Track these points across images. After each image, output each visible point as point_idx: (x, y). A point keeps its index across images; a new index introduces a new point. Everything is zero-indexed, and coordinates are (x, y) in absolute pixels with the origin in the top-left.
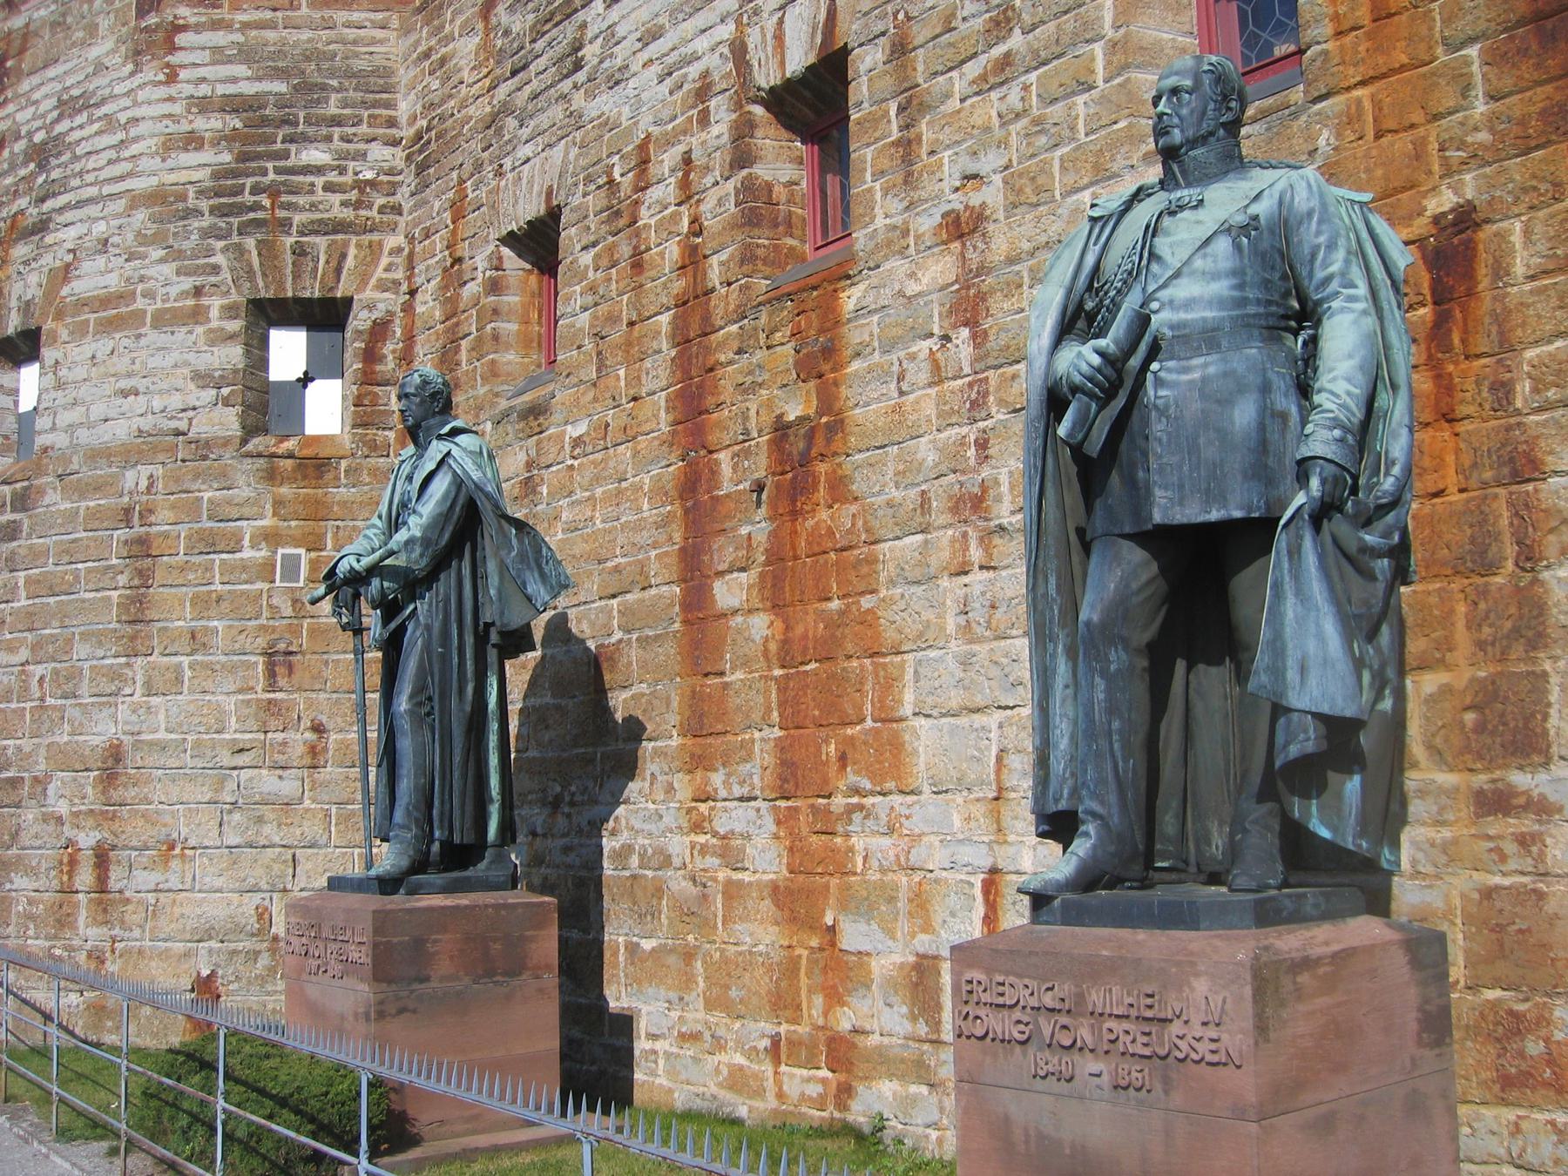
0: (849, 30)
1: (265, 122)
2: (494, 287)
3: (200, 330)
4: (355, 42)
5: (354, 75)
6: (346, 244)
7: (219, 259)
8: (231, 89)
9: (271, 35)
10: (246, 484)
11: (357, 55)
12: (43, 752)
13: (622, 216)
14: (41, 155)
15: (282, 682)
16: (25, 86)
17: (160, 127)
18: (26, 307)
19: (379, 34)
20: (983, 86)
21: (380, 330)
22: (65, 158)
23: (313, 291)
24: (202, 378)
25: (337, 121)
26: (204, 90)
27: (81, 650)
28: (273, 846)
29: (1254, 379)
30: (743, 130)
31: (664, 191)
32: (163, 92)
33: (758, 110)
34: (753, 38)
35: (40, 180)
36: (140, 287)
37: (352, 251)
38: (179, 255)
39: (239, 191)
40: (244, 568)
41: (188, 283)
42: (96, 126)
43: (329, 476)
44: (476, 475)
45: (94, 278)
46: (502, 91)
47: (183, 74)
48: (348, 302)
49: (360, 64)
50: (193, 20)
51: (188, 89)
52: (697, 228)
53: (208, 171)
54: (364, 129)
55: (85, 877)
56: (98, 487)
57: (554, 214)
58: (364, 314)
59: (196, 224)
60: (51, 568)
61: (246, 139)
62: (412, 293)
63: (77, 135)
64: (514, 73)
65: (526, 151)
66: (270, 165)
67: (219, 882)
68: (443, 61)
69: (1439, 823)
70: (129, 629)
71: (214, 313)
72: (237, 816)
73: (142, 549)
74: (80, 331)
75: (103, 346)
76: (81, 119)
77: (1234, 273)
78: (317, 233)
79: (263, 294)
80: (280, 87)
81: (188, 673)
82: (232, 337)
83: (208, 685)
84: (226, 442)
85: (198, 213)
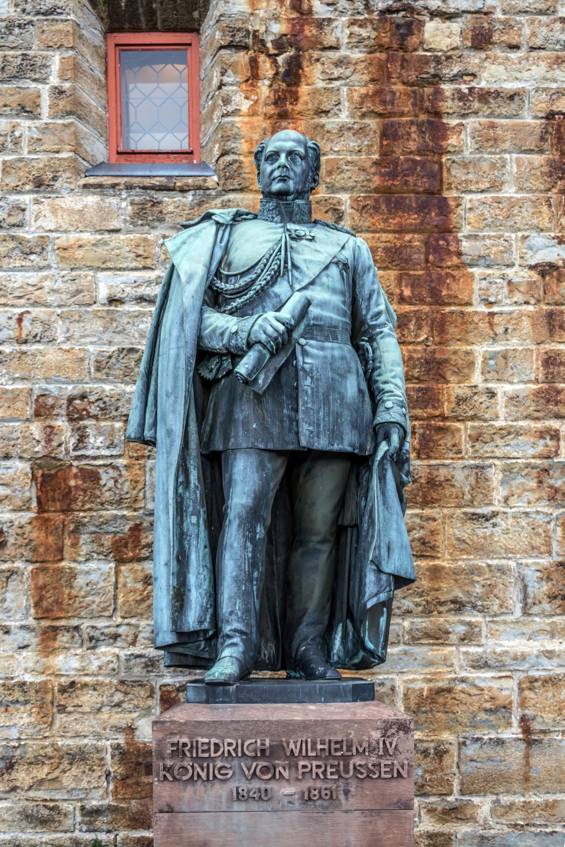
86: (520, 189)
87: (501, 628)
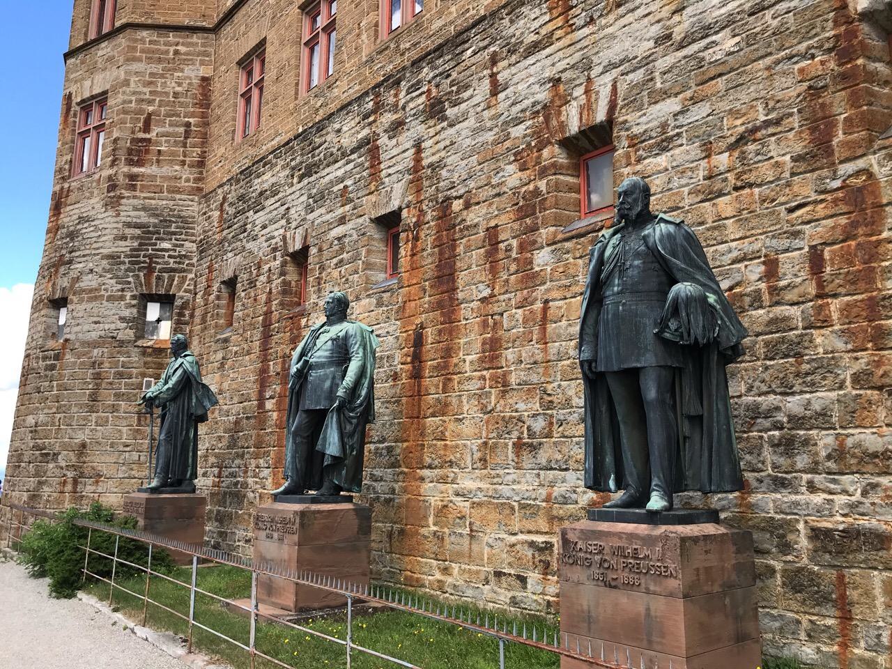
0: (311, 241)
1: (149, 232)
2: (218, 298)
3: (122, 303)
4: (182, 206)
5: (181, 217)
6: (175, 276)
7: (130, 279)
8: (138, 221)
9: (153, 202)
11: (182, 211)
12: (58, 444)
13: (252, 284)
14: (72, 235)
15: (143, 423)
17: (115, 231)
19: (191, 203)
20: (337, 265)
21: (184, 306)
22: (80, 238)
23: (162, 292)
24: (122, 319)
25: (174, 233)
26: (129, 219)
27: (74, 409)
28: (135, 478)
29: (331, 376)
30: (284, 264)
31: (263, 278)
32: (115, 219)
33: (288, 258)
34: (288, 236)
35: (71, 245)
36: (103, 287)
37: (176, 279)
38: (117, 277)
39: (138, 256)
40: (133, 385)
41: (120, 287)
42: (92, 229)
43: (163, 354)
44: (190, 370)
45: (88, 282)
46: (225, 232)
47: (122, 214)
48: (174, 295)
49: (183, 214)
50: (127, 195)
51: (124, 219)
52: (270, 292)
53: (129, 248)
54: (183, 236)
55: (69, 487)
57: (236, 277)
58: (179, 300)
59: (123, 267)
60: (66, 381)
61: (142, 238)
62: (196, 294)
63: (84, 231)
64: (229, 228)
65: (230, 255)
66: (150, 248)
67: (115, 490)
68: (209, 217)
69: (404, 481)
70: (91, 403)
71: (128, 298)
72: (124, 468)
73: (98, 377)
74: (81, 301)
75: (89, 306)
76: (86, 225)
77: (331, 350)
78: (165, 272)
79: (145, 292)
80: (153, 220)
81: (111, 419)
82: (134, 306)
83: (117, 423)
84: (129, 342)
85: (124, 263)
86: (477, 266)
87: (465, 475)
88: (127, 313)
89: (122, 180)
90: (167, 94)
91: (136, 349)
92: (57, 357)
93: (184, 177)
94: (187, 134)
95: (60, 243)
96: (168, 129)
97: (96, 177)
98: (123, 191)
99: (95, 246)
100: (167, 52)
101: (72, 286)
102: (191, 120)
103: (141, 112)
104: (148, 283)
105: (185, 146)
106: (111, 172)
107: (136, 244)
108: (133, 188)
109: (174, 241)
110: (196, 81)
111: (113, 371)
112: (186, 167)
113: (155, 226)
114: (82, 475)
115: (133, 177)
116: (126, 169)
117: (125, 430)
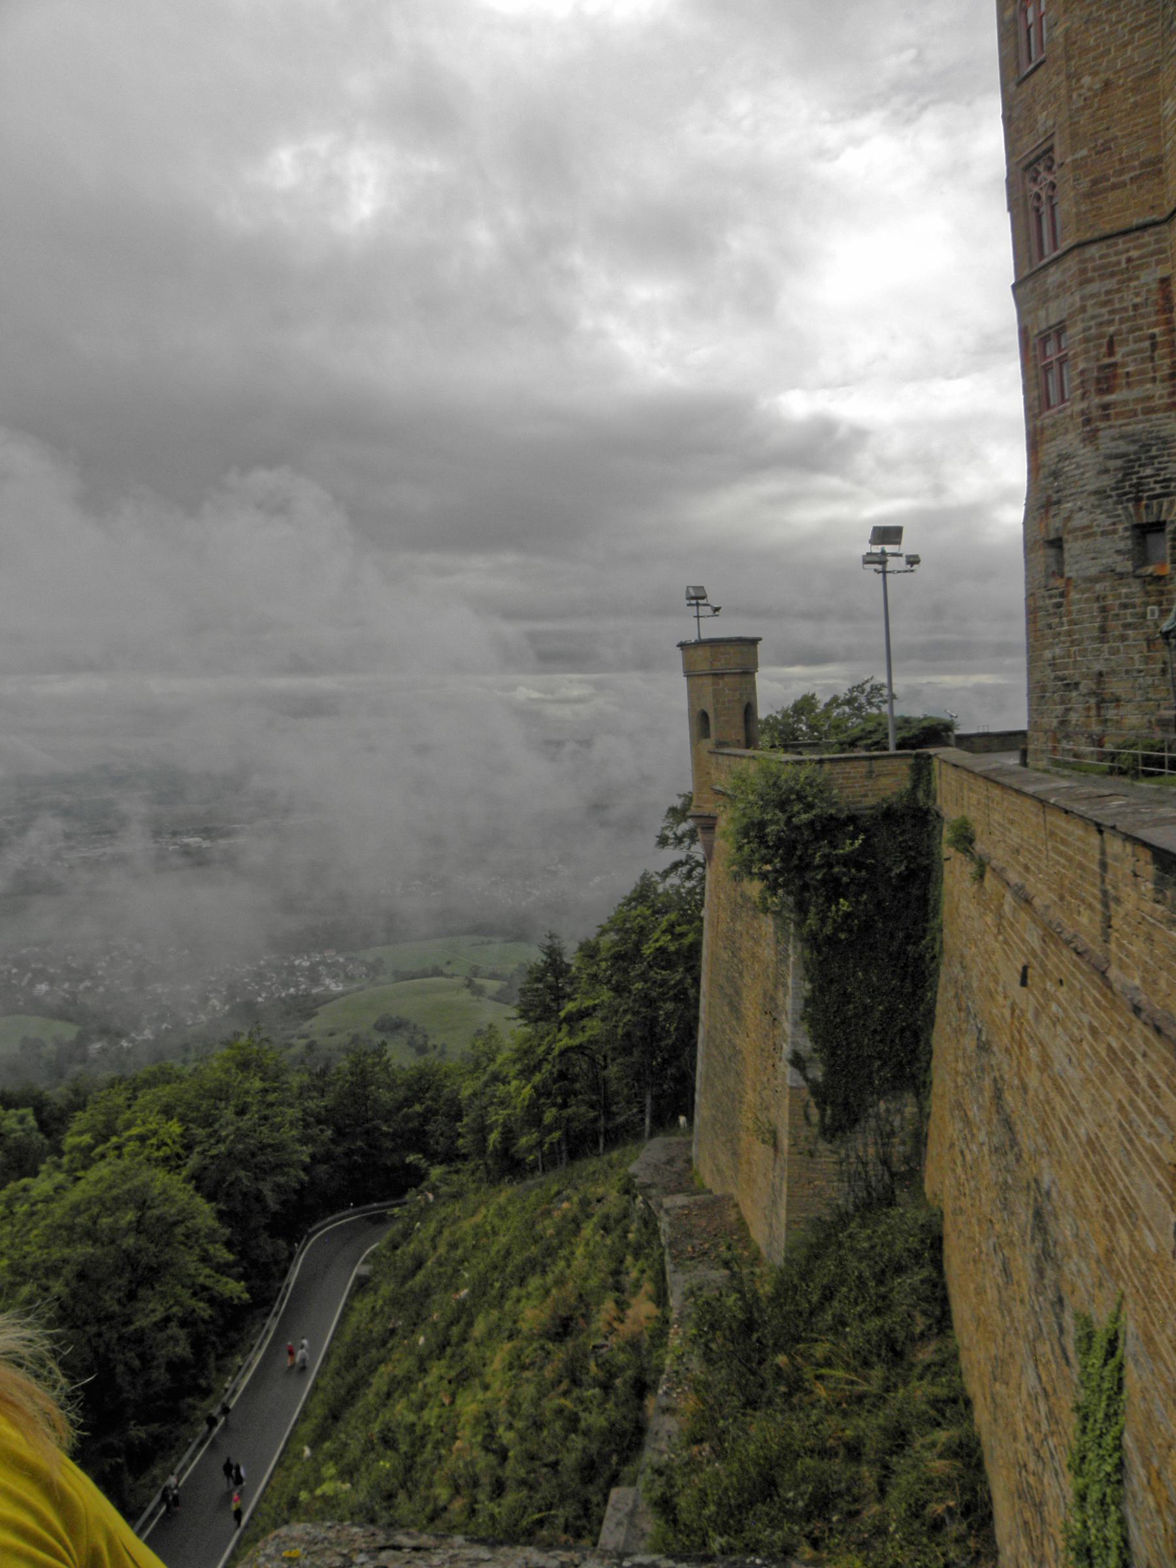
1: (1130, 461)
7: (1120, 512)
10: (1136, 587)
14: (1055, 475)
16: (1046, 446)
18: (1057, 530)
23: (1152, 519)
24: (1118, 552)
27: (1087, 643)
41: (1111, 520)
45: (1080, 520)
47: (1101, 447)
49: (1162, 434)
54: (1166, 459)
55: (1093, 712)
56: (1088, 590)
59: (1110, 501)
73: (1104, 609)
74: (1076, 539)
76: (1067, 463)
80: (1133, 448)
84: (1128, 573)
88: (1121, 545)
89: (1095, 413)
90: (1125, 309)
91: (1138, 581)
92: (1062, 595)
93: (1157, 394)
94: (1154, 346)
95: (1043, 483)
96: (1132, 346)
97: (1069, 412)
98: (1098, 424)
99: (1081, 483)
100: (1119, 263)
101: (1065, 525)
102: (1156, 330)
103: (1101, 336)
104: (1137, 513)
105: (1152, 359)
106: (1083, 405)
107: (1120, 476)
108: (1107, 417)
109: (1157, 465)
110: (1154, 286)
111: (1117, 602)
112: (1158, 383)
113: (1135, 453)
114: (1103, 701)
115: (1105, 407)
116: (1097, 400)
117: (1137, 657)
